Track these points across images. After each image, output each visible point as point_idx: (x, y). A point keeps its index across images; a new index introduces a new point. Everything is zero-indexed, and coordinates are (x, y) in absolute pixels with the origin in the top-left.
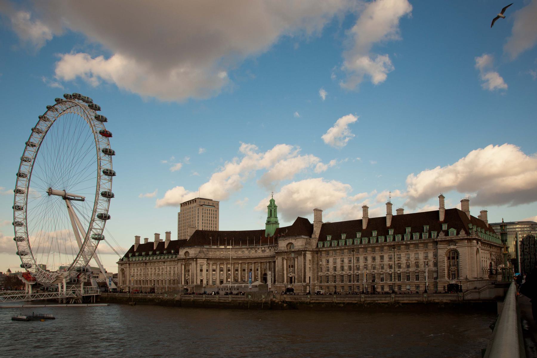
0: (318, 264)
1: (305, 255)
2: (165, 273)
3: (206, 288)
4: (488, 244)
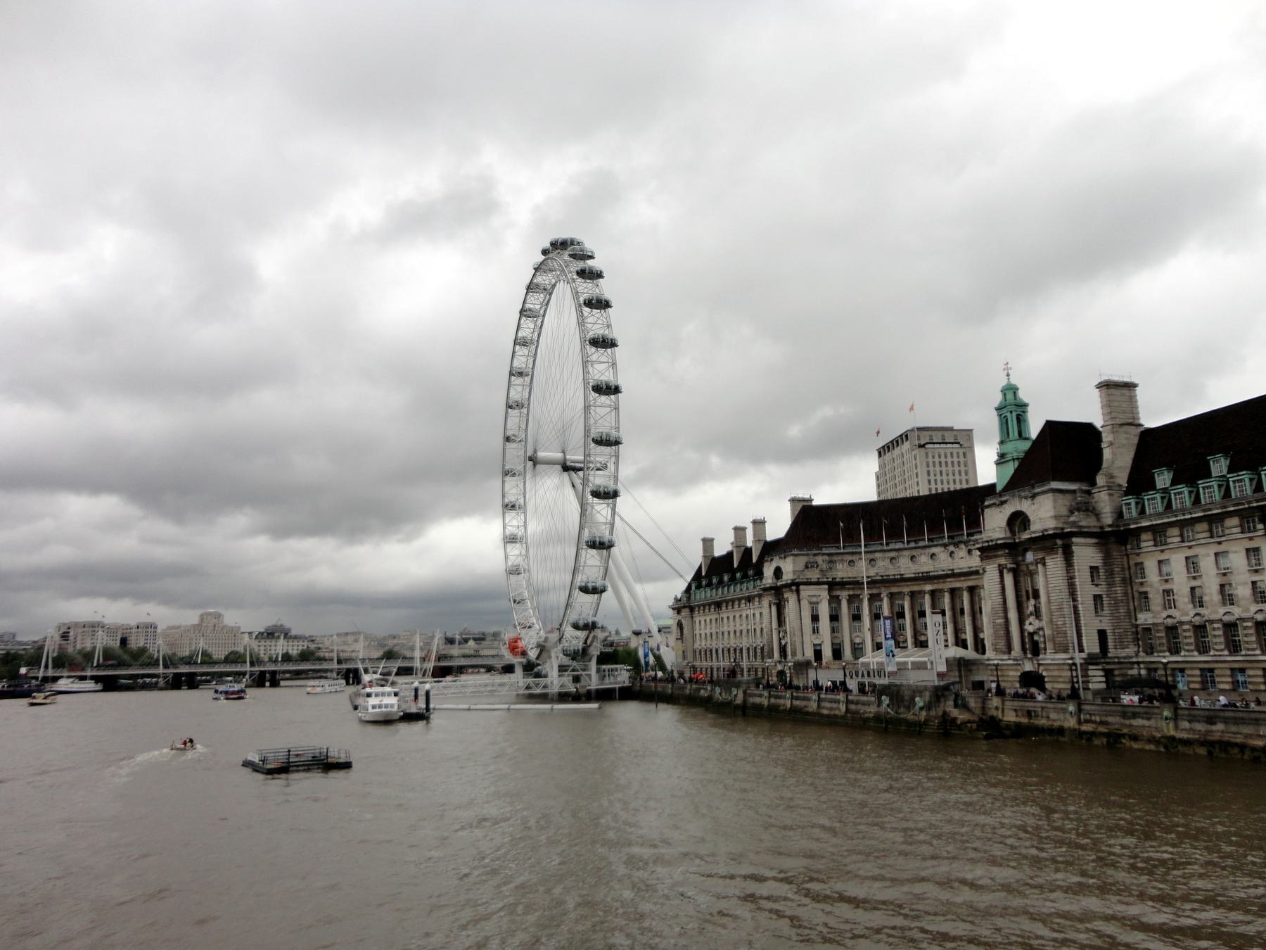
0: (1128, 582)
3: (818, 670)
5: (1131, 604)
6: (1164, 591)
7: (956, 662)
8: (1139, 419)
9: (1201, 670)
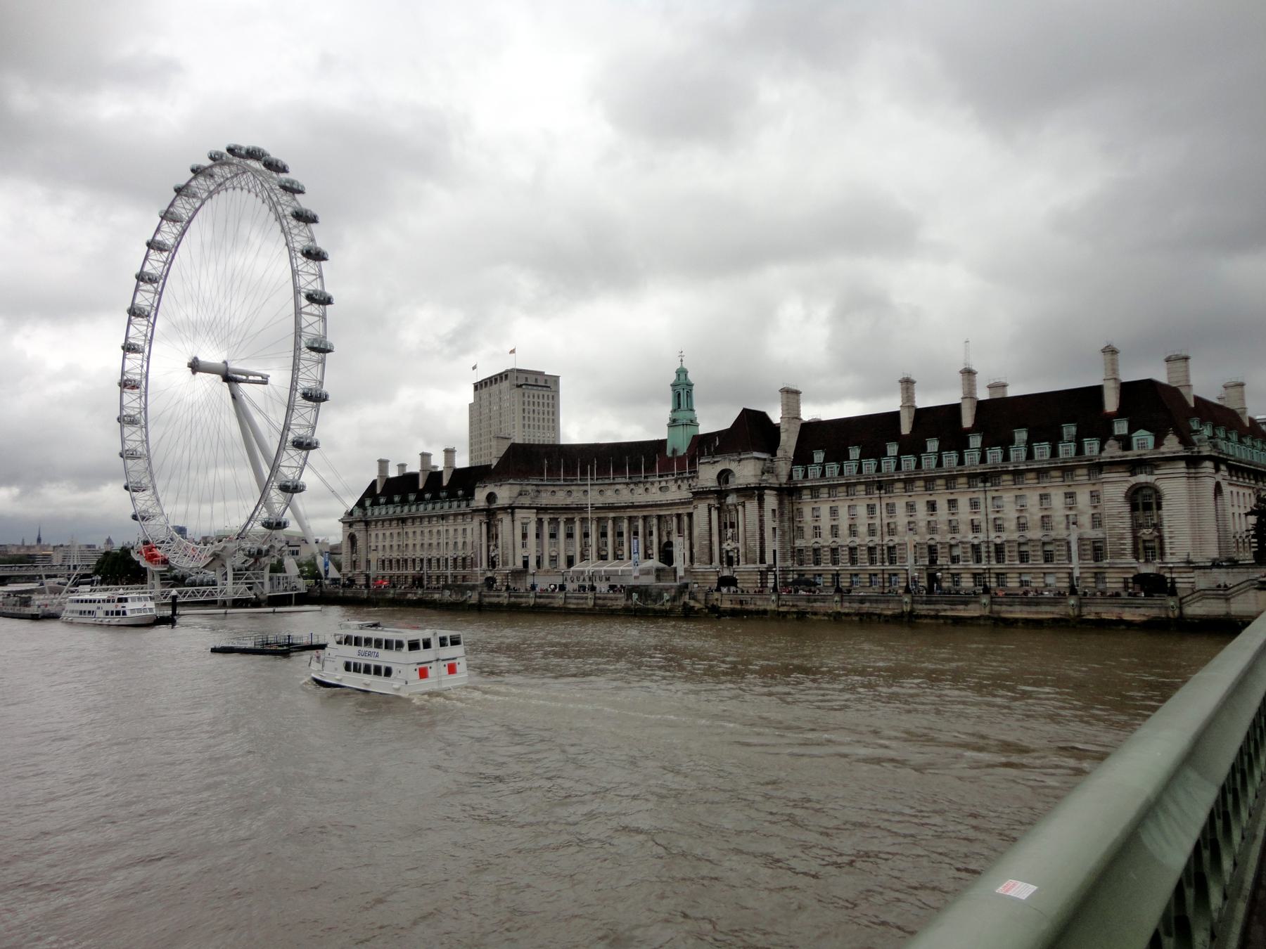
0: (792, 520)
2: (445, 541)
4: (1249, 471)
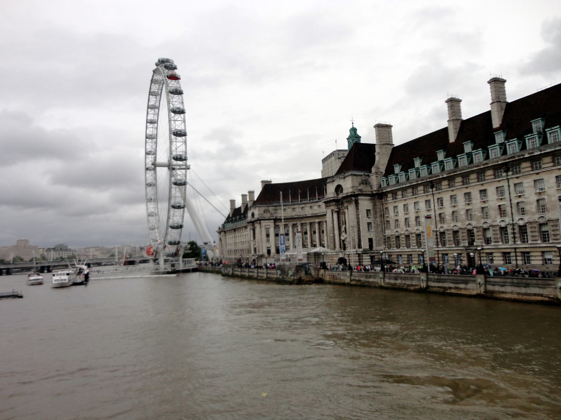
0: (382, 216)
1: (357, 203)
5: (383, 226)
6: (395, 220)
7: (314, 254)
8: (392, 142)
9: (408, 255)
